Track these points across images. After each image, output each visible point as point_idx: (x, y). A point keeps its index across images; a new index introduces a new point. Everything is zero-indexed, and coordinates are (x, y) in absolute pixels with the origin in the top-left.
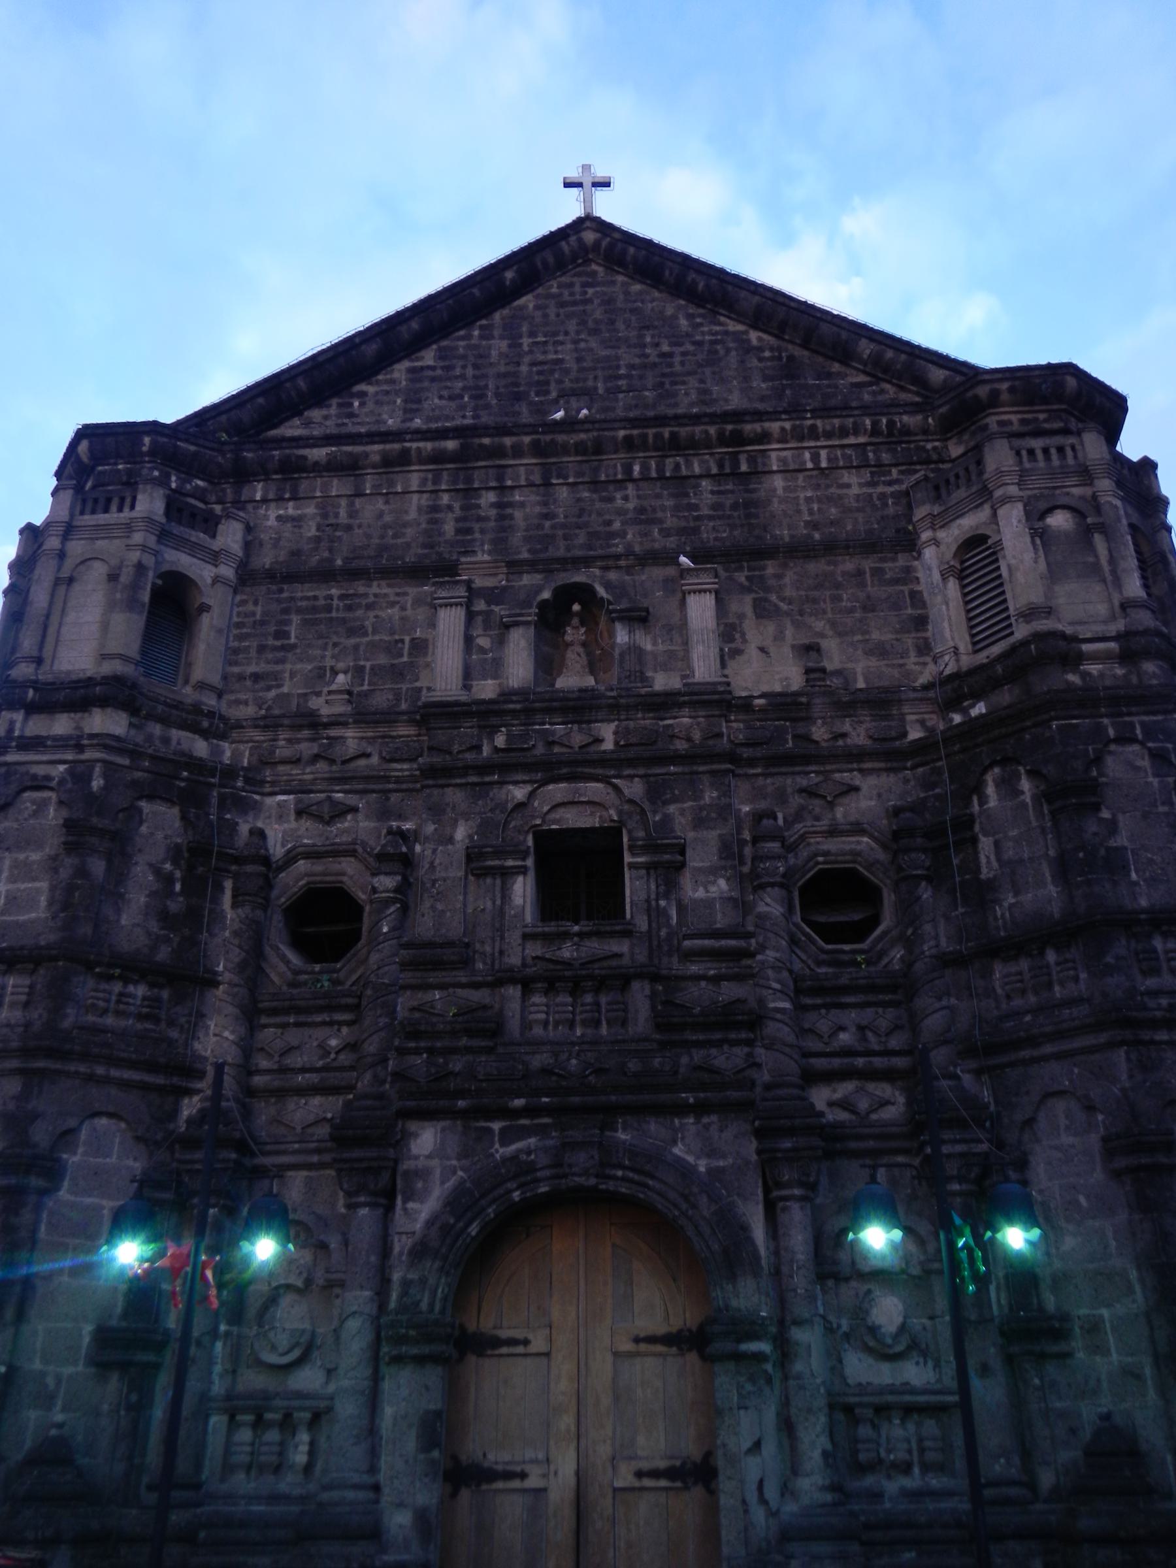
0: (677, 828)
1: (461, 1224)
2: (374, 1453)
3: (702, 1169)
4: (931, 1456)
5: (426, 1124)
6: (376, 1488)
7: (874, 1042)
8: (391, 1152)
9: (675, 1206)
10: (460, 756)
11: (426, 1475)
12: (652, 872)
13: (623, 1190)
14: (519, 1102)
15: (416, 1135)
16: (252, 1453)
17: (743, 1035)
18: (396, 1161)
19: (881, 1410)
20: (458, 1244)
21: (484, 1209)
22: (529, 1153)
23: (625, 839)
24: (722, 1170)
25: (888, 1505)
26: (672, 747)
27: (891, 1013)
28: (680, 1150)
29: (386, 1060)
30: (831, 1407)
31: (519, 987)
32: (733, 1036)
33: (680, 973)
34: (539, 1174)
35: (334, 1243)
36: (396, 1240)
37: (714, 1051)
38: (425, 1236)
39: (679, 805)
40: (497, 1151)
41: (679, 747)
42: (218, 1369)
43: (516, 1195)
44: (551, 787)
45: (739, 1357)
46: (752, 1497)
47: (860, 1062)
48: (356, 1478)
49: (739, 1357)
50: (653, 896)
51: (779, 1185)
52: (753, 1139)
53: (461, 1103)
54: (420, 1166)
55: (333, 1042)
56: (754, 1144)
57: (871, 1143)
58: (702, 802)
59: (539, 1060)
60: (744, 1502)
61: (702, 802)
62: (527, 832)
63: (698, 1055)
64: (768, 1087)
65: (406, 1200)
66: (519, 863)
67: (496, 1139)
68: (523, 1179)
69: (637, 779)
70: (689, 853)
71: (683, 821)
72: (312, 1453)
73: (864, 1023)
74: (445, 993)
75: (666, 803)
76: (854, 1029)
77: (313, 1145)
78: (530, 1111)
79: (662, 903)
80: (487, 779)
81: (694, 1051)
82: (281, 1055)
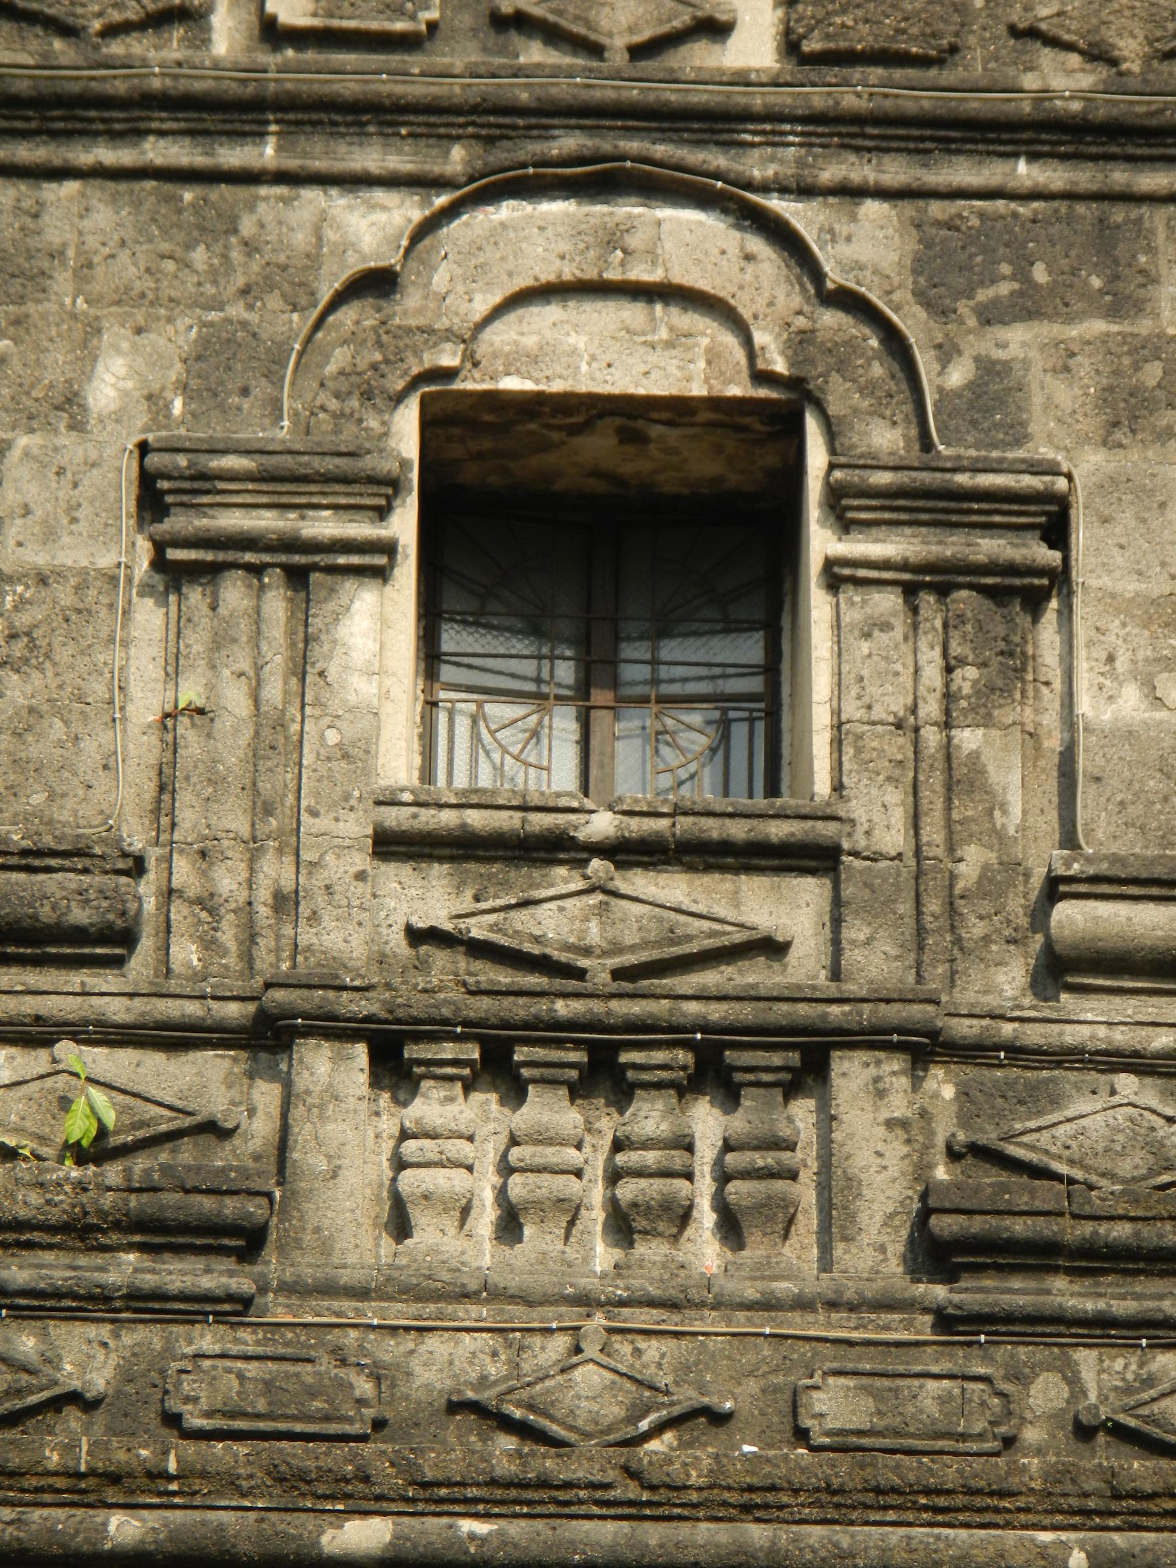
0: (1040, 424)
10: (116, 48)
12: (927, 600)
23: (816, 457)
26: (1030, 81)
31: (361, 1052)
33: (1034, 1035)
39: (1047, 330)
41: (1058, 82)
44: (508, 210)
50: (931, 708)
58: (1144, 326)
61: (1144, 326)
62: (399, 399)
66: (361, 529)
69: (872, 208)
70: (1082, 535)
71: (1065, 395)
74: (36, 1061)
75: (989, 317)
79: (968, 739)
80: (232, 156)
81: (1086, 1359)
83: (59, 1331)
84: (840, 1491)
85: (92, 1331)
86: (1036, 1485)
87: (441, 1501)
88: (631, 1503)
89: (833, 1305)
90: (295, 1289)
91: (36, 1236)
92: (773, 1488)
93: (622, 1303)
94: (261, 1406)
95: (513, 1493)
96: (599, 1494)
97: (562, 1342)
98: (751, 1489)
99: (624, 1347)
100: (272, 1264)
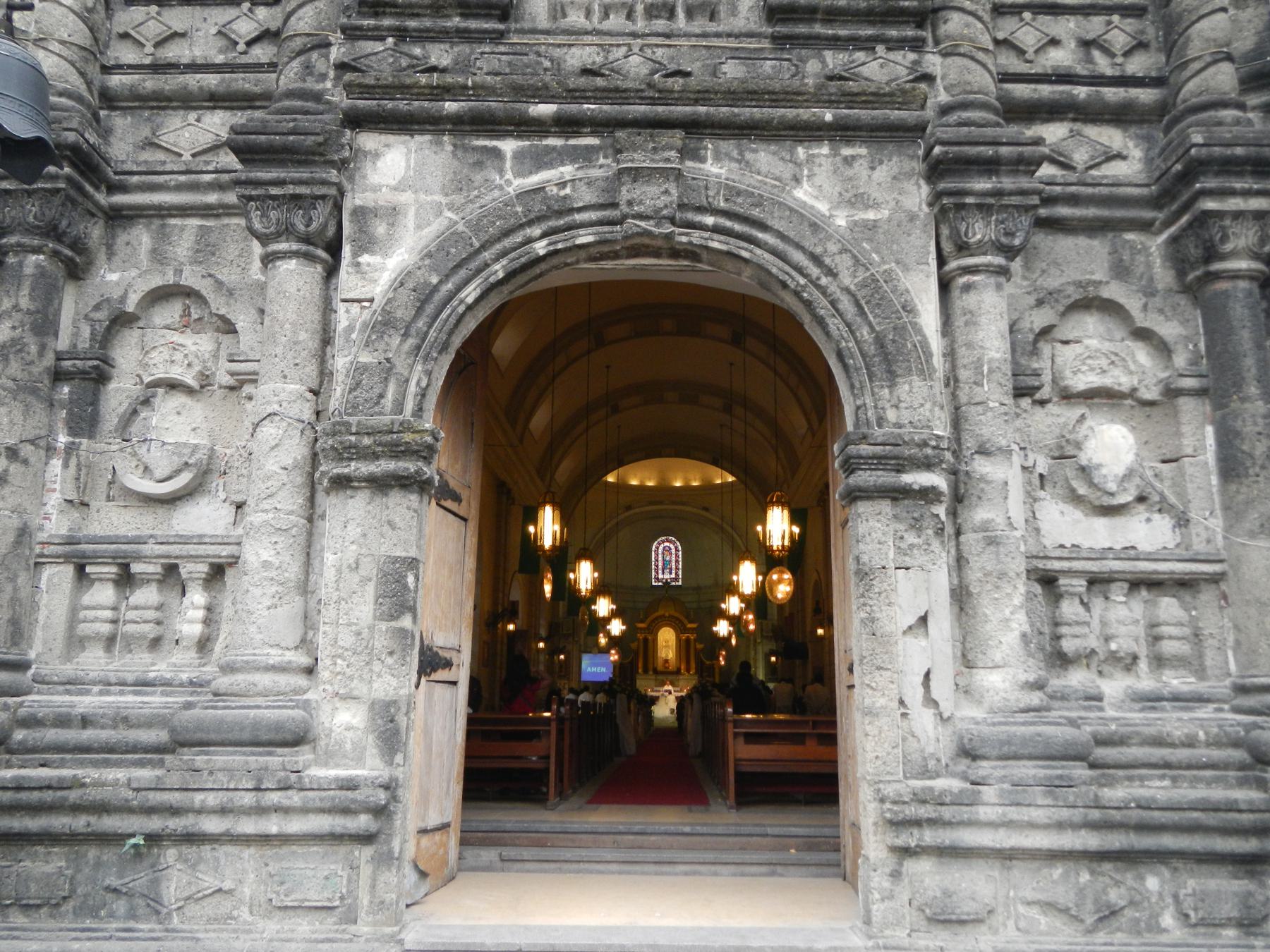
1: (450, 286)
2: (308, 621)
3: (841, 221)
4: (1168, 647)
5: (391, 138)
6: (310, 671)
7: (1103, 65)
8: (333, 175)
9: (800, 270)
11: (391, 653)
13: (716, 245)
14: (545, 109)
15: (377, 155)
16: (114, 622)
17: (910, 32)
18: (342, 193)
19: (1097, 582)
20: (444, 315)
21: (487, 265)
22: (563, 185)
24: (872, 226)
25: (1110, 713)
27: (1131, 24)
28: (806, 192)
29: (328, 45)
30: (1028, 571)
32: (893, 33)
34: (578, 217)
35: (243, 321)
36: (341, 307)
37: (860, 56)
38: (389, 301)
40: (509, 183)
42: (54, 500)
43: (541, 248)
45: (898, 494)
46: (914, 695)
47: (1082, 92)
48: (275, 656)
49: (898, 494)
51: (963, 248)
52: (922, 182)
53: (450, 107)
54: (381, 203)
55: (245, 28)
56: (925, 189)
57: (1091, 212)
59: (578, 57)
60: (902, 702)
63: (834, 60)
64: (945, 110)
65: (359, 250)
67: (508, 164)
68: (553, 223)
72: (207, 622)
73: (1090, 36)
76: (1073, 45)
77: (207, 178)
78: (567, 125)
81: (828, 55)
82: (157, 45)
83: (429, 46)
84: (733, 93)
85: (442, 46)
86: (812, 90)
87: (576, 98)
88: (651, 98)
89: (729, 35)
90: (522, 32)
91: (420, 11)
92: (707, 91)
93: (648, 35)
94: (507, 70)
95: (605, 94)
96: (640, 94)
97: (624, 50)
98: (699, 92)
99: (649, 52)
100: (513, 26)
